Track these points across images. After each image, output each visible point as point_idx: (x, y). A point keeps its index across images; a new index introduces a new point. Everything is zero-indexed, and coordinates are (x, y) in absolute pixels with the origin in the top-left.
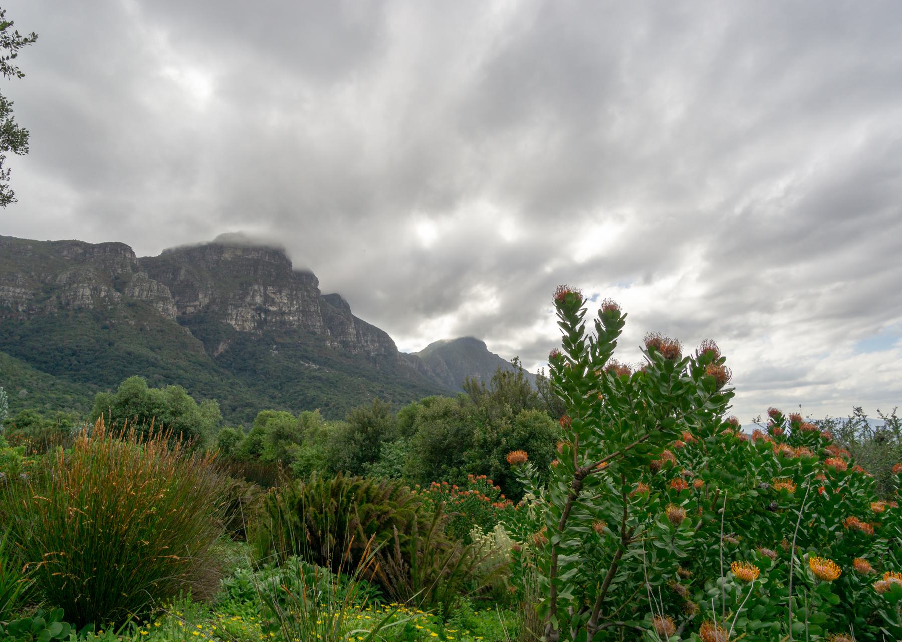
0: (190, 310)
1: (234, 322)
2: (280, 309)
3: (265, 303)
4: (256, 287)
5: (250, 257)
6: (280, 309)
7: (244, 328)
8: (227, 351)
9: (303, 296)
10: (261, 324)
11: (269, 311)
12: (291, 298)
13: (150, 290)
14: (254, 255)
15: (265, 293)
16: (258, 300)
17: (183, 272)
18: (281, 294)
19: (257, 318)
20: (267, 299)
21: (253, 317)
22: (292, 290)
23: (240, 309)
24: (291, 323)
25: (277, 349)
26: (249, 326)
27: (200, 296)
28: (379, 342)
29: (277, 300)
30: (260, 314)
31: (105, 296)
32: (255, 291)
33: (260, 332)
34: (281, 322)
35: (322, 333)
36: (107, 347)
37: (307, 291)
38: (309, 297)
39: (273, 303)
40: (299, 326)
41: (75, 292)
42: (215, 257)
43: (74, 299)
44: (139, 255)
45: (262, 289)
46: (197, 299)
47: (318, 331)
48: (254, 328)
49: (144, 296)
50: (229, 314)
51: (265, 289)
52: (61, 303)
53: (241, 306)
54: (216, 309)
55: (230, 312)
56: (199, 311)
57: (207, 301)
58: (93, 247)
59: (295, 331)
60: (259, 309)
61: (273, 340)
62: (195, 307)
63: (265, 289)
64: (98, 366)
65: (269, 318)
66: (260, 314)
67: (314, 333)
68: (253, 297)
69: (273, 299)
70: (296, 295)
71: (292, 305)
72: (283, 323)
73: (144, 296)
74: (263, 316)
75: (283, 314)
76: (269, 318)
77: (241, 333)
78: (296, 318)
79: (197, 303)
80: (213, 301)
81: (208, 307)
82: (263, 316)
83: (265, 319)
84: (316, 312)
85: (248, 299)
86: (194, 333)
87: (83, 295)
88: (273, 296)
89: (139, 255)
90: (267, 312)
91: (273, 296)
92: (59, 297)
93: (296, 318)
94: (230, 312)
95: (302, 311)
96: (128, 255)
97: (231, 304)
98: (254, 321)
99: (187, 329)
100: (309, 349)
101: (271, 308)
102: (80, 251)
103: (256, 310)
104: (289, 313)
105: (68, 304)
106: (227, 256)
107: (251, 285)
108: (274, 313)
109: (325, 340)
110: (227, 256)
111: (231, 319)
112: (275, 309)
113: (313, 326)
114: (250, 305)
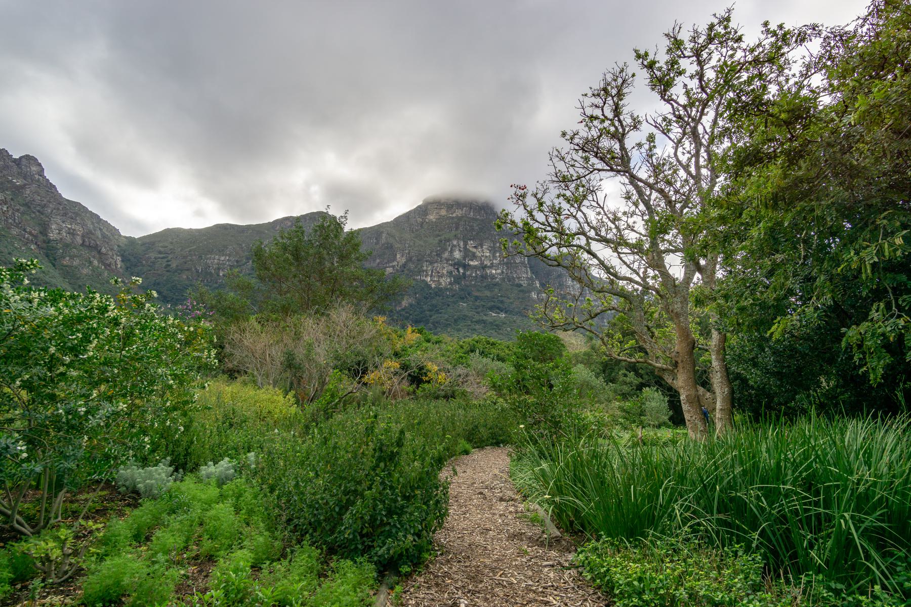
2: (482, 263)
3: (464, 259)
4: (455, 243)
5: (454, 215)
6: (482, 263)
7: (440, 284)
10: (458, 279)
11: (469, 265)
12: (493, 250)
14: (459, 213)
15: (465, 248)
16: (457, 255)
17: (384, 235)
23: (436, 265)
26: (445, 282)
27: (398, 256)
32: (454, 246)
35: (529, 285)
39: (474, 257)
40: (503, 279)
45: (462, 244)
46: (395, 259)
47: (524, 283)
48: (450, 283)
50: (423, 271)
51: (466, 244)
55: (425, 268)
57: (404, 260)
59: (496, 284)
60: (458, 264)
62: (393, 267)
63: (466, 244)
65: (468, 273)
67: (520, 286)
68: (451, 252)
69: (474, 254)
71: (494, 257)
72: (484, 277)
74: (461, 271)
75: (484, 267)
78: (499, 271)
79: (395, 263)
80: (410, 260)
81: (404, 266)
82: (461, 271)
83: (464, 274)
84: (523, 263)
85: (446, 255)
88: (474, 250)
90: (465, 267)
91: (474, 250)
93: (499, 271)
94: (425, 268)
95: (507, 264)
101: (471, 263)
103: (453, 265)
106: (432, 217)
107: (449, 240)
108: (475, 267)
109: (530, 292)
110: (432, 217)
112: (476, 263)
113: (519, 278)
114: (448, 260)
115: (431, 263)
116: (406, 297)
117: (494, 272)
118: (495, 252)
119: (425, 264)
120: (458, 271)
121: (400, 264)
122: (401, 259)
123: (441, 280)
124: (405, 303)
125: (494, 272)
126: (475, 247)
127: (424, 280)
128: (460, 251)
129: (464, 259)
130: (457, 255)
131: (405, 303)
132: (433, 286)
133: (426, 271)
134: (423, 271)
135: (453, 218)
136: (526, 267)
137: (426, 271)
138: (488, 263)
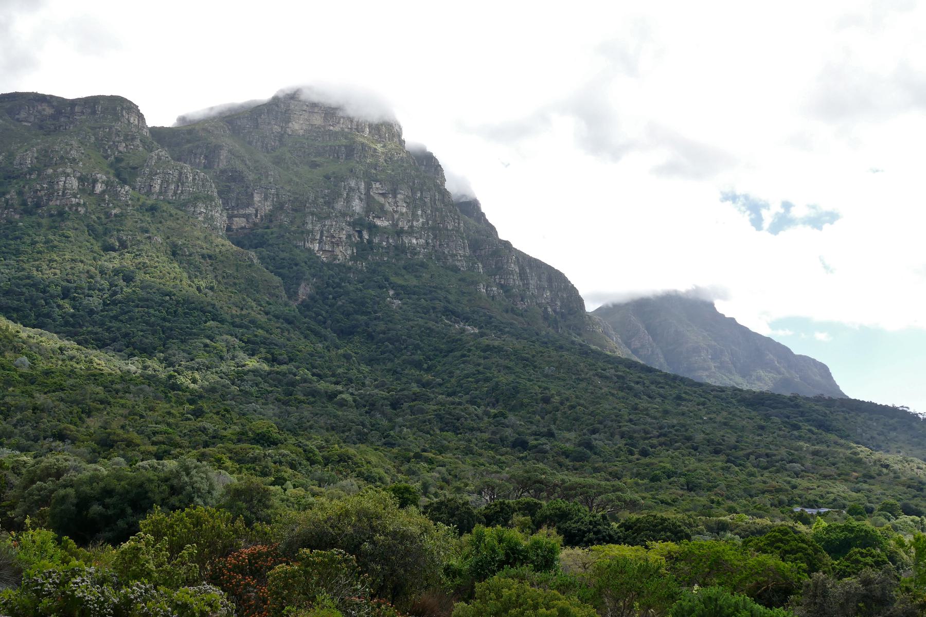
1: (316, 247)
2: (395, 225)
4: (353, 184)
6: (395, 225)
8: (311, 298)
9: (433, 200)
10: (363, 250)
11: (376, 226)
12: (412, 204)
13: (180, 181)
15: (367, 194)
16: (357, 206)
17: (224, 154)
18: (395, 197)
19: (355, 239)
20: (370, 205)
21: (349, 236)
23: (327, 222)
25: (397, 296)
26: (343, 253)
27: (257, 198)
29: (388, 208)
30: (360, 232)
31: (103, 192)
32: (351, 189)
33: (362, 265)
34: (396, 247)
36: (122, 283)
38: (443, 202)
41: (51, 184)
42: (276, 129)
43: (50, 196)
44: (151, 122)
45: (362, 186)
47: (462, 265)
48: (352, 258)
49: (170, 193)
50: (308, 232)
51: (368, 188)
52: (24, 203)
53: (328, 217)
54: (286, 221)
55: (310, 227)
56: (255, 224)
57: (268, 207)
58: (74, 103)
59: (423, 265)
60: (359, 224)
61: (387, 280)
63: (368, 188)
64: (115, 318)
66: (360, 232)
67: (456, 270)
68: (348, 200)
69: (382, 207)
70: (421, 199)
72: (400, 250)
73: (170, 193)
75: (400, 233)
76: (376, 240)
77: (329, 265)
78: (422, 241)
79: (251, 211)
82: (366, 236)
83: (370, 241)
85: (340, 205)
86: (262, 258)
87: (65, 189)
89: (151, 122)
90: (372, 228)
92: (20, 193)
93: (422, 241)
94: (310, 227)
95: (433, 229)
96: (134, 120)
97: (313, 214)
98: (351, 245)
99: (252, 254)
100: (451, 298)
101: (378, 223)
102: (49, 111)
103: (353, 224)
104: (411, 232)
105: (38, 205)
108: (384, 230)
110: (297, 126)
112: (386, 223)
113: (453, 256)
114: (344, 215)
115: (321, 218)
117: (414, 241)
119: (309, 219)
120: (361, 236)
121: (261, 213)
123: (339, 251)
125: (414, 241)
126: (383, 195)
127: (309, 250)
128: (361, 199)
136: (463, 238)
138: (404, 225)
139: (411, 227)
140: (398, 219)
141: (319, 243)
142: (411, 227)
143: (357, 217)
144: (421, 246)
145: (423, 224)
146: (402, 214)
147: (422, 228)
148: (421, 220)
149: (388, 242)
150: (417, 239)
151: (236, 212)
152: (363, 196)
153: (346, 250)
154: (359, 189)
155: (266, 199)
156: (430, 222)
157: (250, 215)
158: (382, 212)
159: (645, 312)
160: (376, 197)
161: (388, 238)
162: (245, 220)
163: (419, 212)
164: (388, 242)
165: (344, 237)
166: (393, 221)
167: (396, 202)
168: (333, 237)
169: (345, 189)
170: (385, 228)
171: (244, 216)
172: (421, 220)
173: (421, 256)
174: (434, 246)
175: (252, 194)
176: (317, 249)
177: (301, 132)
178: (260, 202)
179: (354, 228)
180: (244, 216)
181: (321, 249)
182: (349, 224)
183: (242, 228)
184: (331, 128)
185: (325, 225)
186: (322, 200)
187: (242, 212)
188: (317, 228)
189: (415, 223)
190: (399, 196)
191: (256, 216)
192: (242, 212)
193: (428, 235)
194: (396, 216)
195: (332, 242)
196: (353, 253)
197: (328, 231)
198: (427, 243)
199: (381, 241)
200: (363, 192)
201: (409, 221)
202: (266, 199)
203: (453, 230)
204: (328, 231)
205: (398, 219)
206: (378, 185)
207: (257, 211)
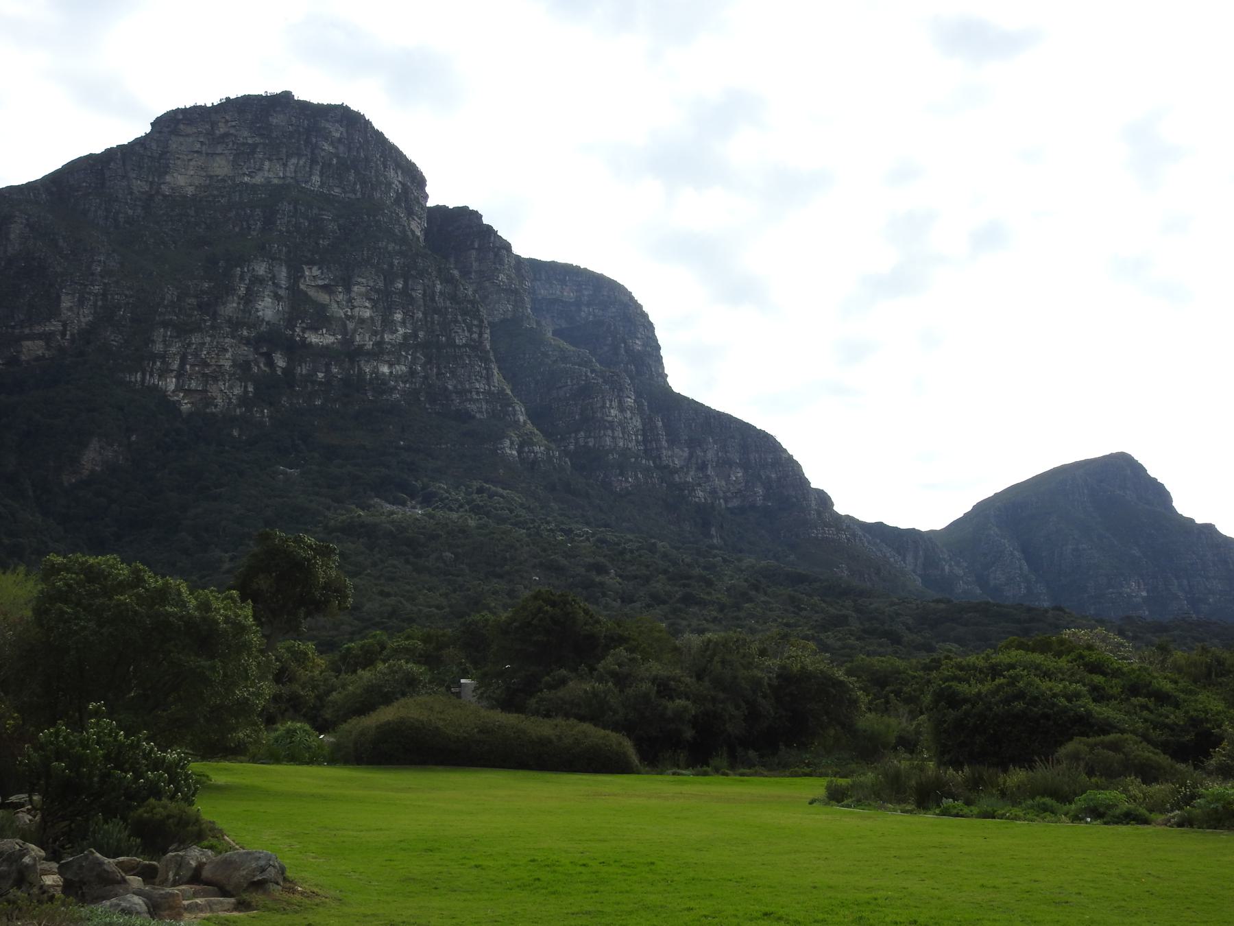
0: (32, 349)
1: (171, 384)
2: (347, 341)
4: (261, 269)
5: (258, 179)
6: (347, 341)
7: (210, 402)
9: (429, 296)
11: (305, 345)
12: (384, 301)
15: (293, 289)
16: (268, 309)
18: (348, 290)
20: (302, 308)
22: (389, 278)
23: (195, 339)
24: (381, 385)
26: (226, 394)
27: (66, 303)
28: (745, 466)
29: (337, 311)
32: (259, 280)
37: (449, 280)
39: (321, 320)
42: (140, 186)
45: (283, 274)
48: (244, 400)
50: (153, 357)
51: (296, 275)
55: (159, 347)
57: (85, 317)
60: (270, 340)
62: (47, 337)
63: (296, 275)
65: (303, 370)
67: (465, 416)
68: (249, 299)
69: (324, 307)
70: (405, 292)
71: (388, 324)
74: (281, 362)
75: (352, 354)
78: (401, 369)
79: (54, 326)
82: (281, 362)
83: (288, 371)
85: (231, 307)
88: (324, 298)
90: (296, 350)
91: (324, 298)
93: (401, 369)
94: (159, 347)
97: (165, 325)
101: (314, 339)
104: (378, 353)
106: (181, 180)
110: (183, 179)
111: (162, 374)
112: (329, 340)
114: (235, 325)
115: (183, 331)
116: (95, 444)
117: (385, 369)
118: (390, 310)
120: (271, 363)
122: (74, 313)
123: (214, 390)
124: (93, 457)
125: (385, 369)
126: (326, 288)
128: (277, 297)
129: (291, 325)
130: (268, 309)
131: (93, 457)
132: (186, 407)
133: (163, 357)
134: (153, 357)
135: (254, 188)
137: (163, 357)
138: (365, 340)
139: (379, 344)
140: (355, 331)
141: (178, 377)
142: (379, 344)
143: (264, 328)
144: (398, 378)
145: (405, 336)
146: (362, 321)
147: (404, 345)
148: (401, 331)
149: (328, 371)
150: (391, 365)
151: (27, 331)
152: (282, 292)
153: (231, 387)
154: (274, 277)
155: (81, 303)
156: (421, 334)
157: (52, 334)
158: (321, 320)
159: (1017, 516)
160: (312, 293)
161: (328, 365)
162: (42, 343)
163: (398, 316)
164: (328, 371)
165: (228, 365)
166: (344, 332)
167: (350, 300)
168: (206, 365)
169: (242, 279)
170: (327, 347)
171: (40, 336)
172: (401, 331)
173: (396, 396)
174: (426, 378)
175: (59, 297)
176: (172, 387)
177: (190, 191)
178: (70, 309)
179: (256, 351)
180: (40, 336)
181: (179, 388)
182: (248, 342)
183: (38, 359)
184: (246, 179)
185: (189, 344)
186: (193, 301)
187: (38, 329)
188: (173, 350)
189: (387, 337)
190: (355, 288)
191: (63, 334)
192: (38, 329)
193: (415, 358)
194: (351, 326)
195: (204, 375)
196: (246, 392)
197: (196, 355)
198: (412, 373)
199: (315, 371)
200: (284, 283)
201: (375, 333)
202: (81, 303)
203: (465, 346)
204: (196, 355)
205: (355, 331)
206: (316, 271)
207: (65, 325)
